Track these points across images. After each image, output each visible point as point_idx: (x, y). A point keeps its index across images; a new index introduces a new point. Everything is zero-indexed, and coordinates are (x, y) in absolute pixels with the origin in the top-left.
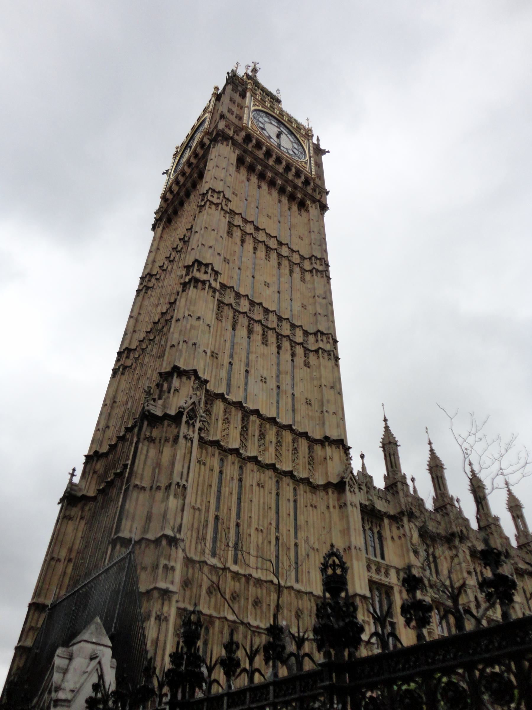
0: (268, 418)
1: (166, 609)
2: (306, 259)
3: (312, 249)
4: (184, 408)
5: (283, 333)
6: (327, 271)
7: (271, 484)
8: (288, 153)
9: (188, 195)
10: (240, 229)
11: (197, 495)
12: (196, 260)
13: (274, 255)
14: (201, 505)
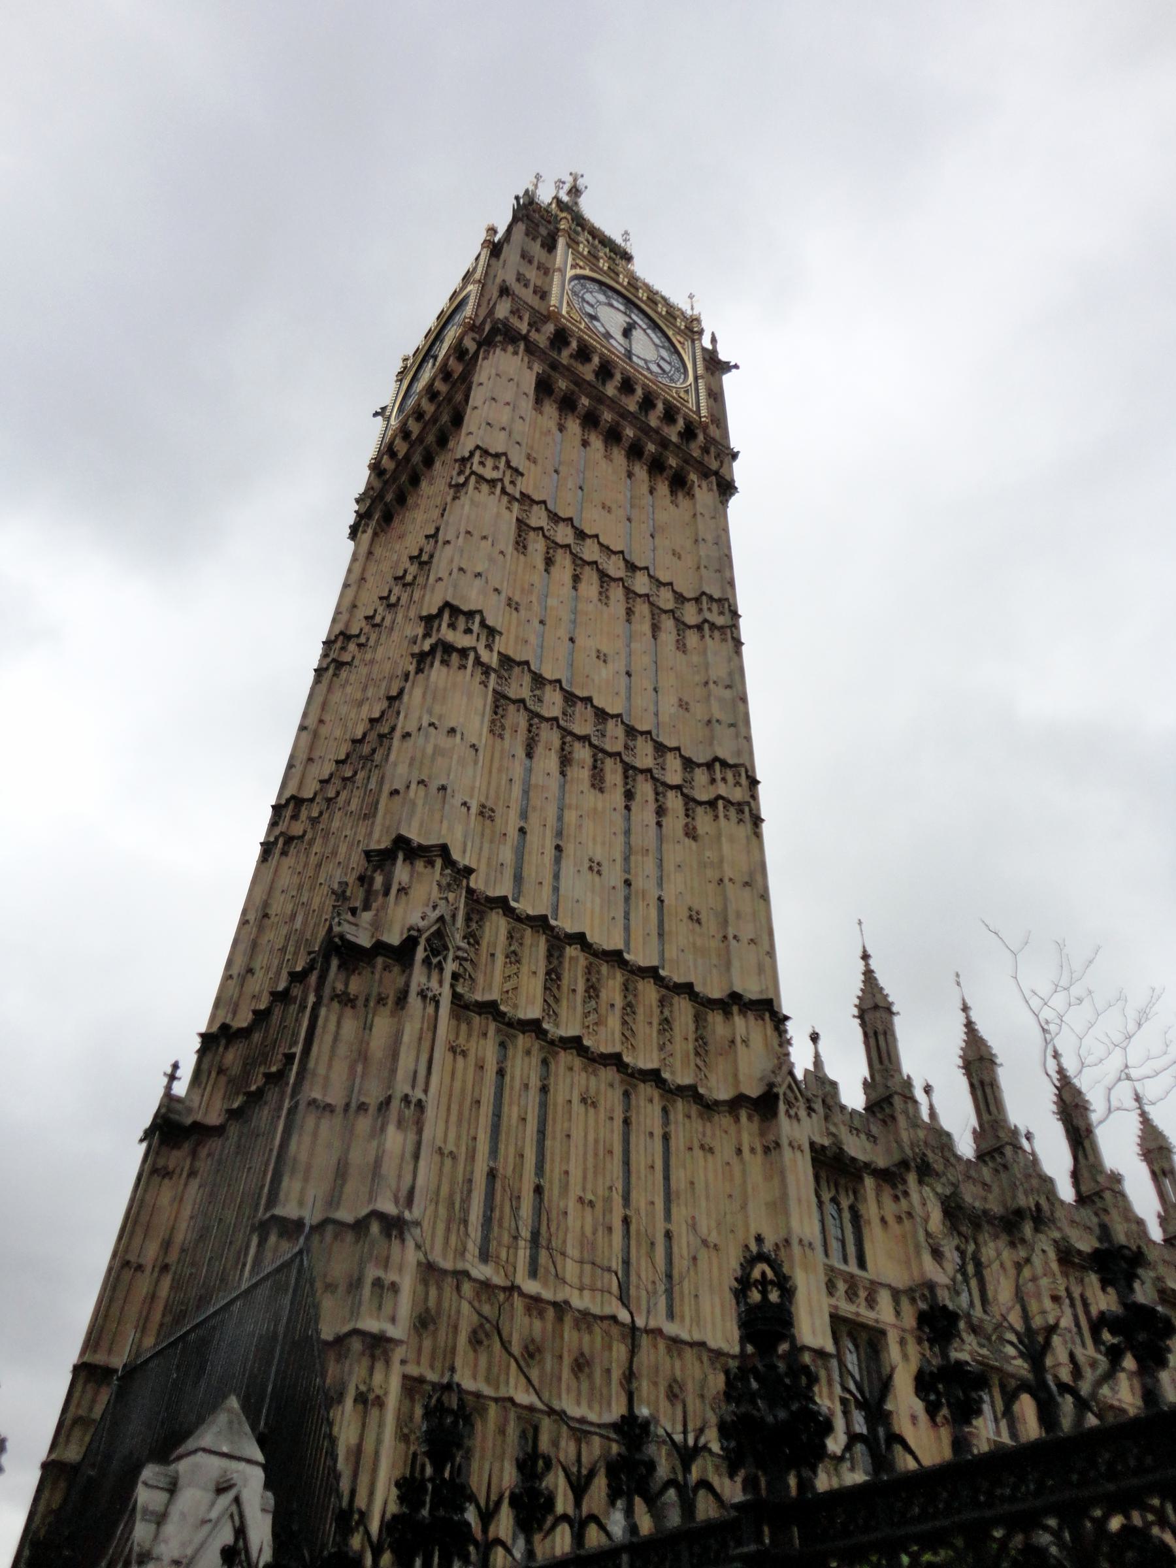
1: (378, 1377)
2: (689, 600)
3: (701, 578)
4: (419, 930)
5: (638, 765)
6: (735, 626)
7: (612, 1099)
8: (648, 369)
9: (429, 462)
10: (544, 536)
11: (447, 1121)
12: (447, 604)
13: (617, 593)
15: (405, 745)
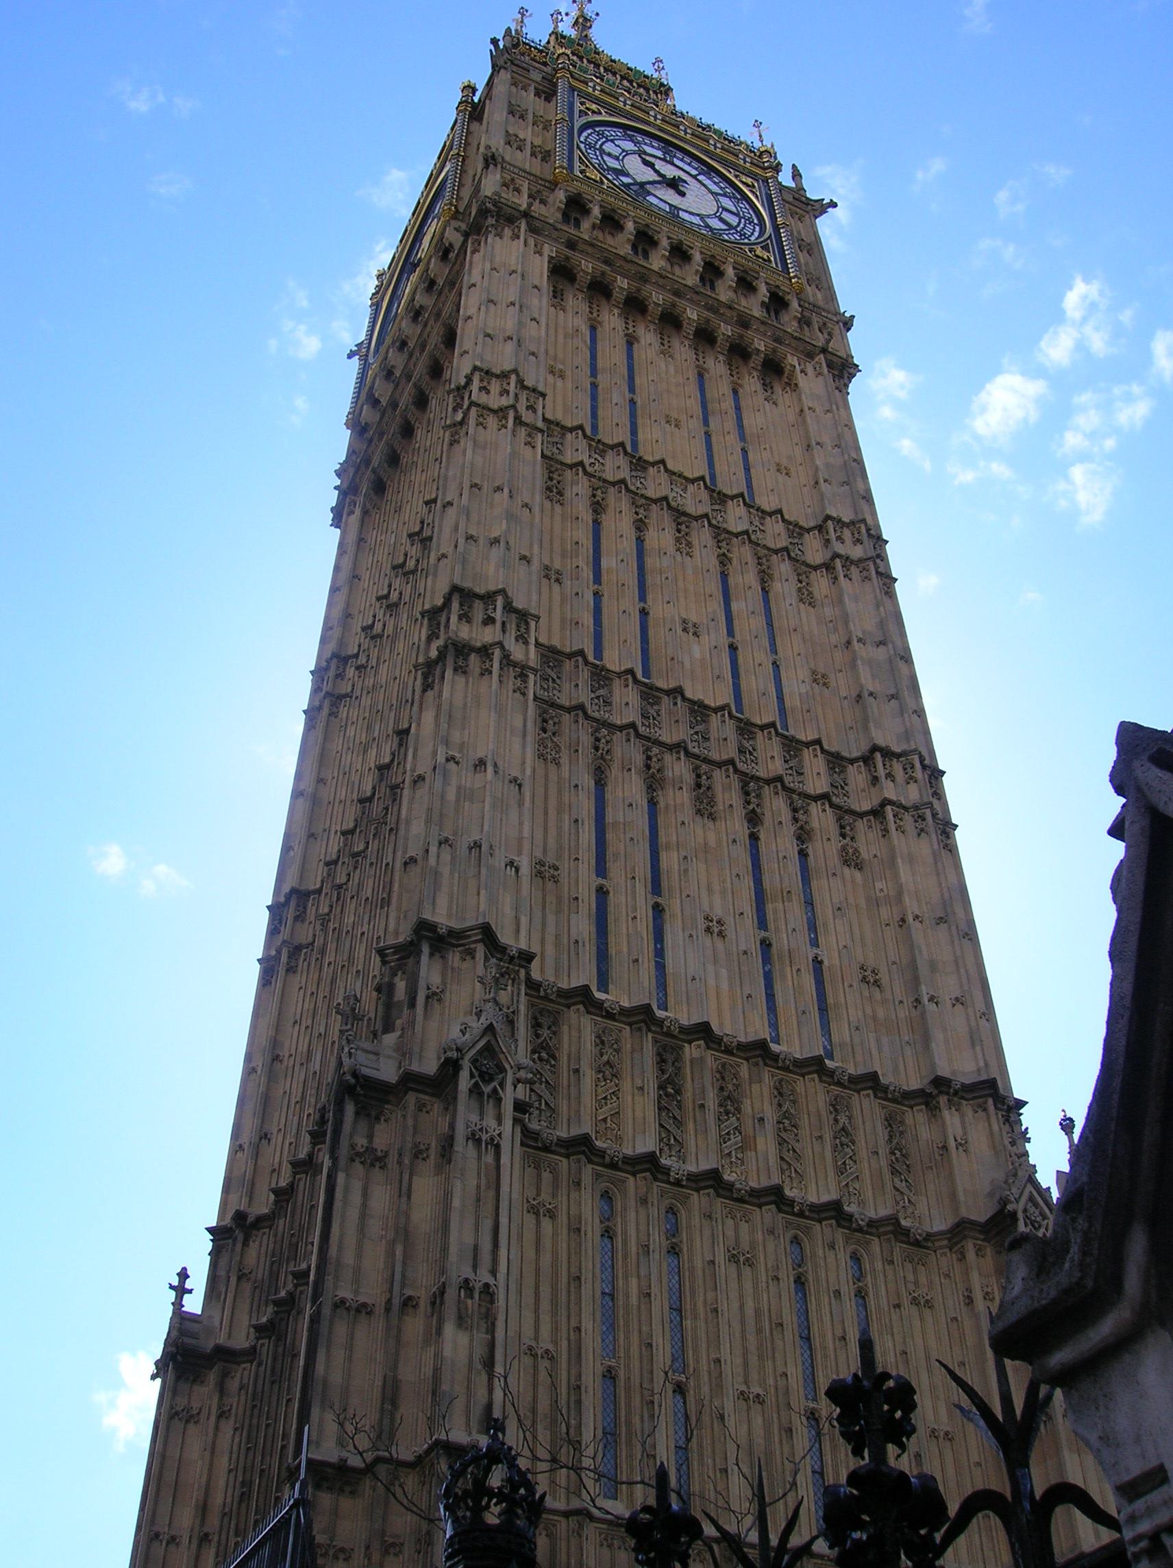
0: (741, 1047)
2: (808, 530)
3: (822, 496)
4: (458, 1050)
5: (762, 773)
6: (881, 557)
7: (773, 1252)
8: (707, 226)
9: (421, 401)
10: (585, 472)
11: (537, 1311)
13: (702, 536)
14: (555, 1342)
15: (419, 793)
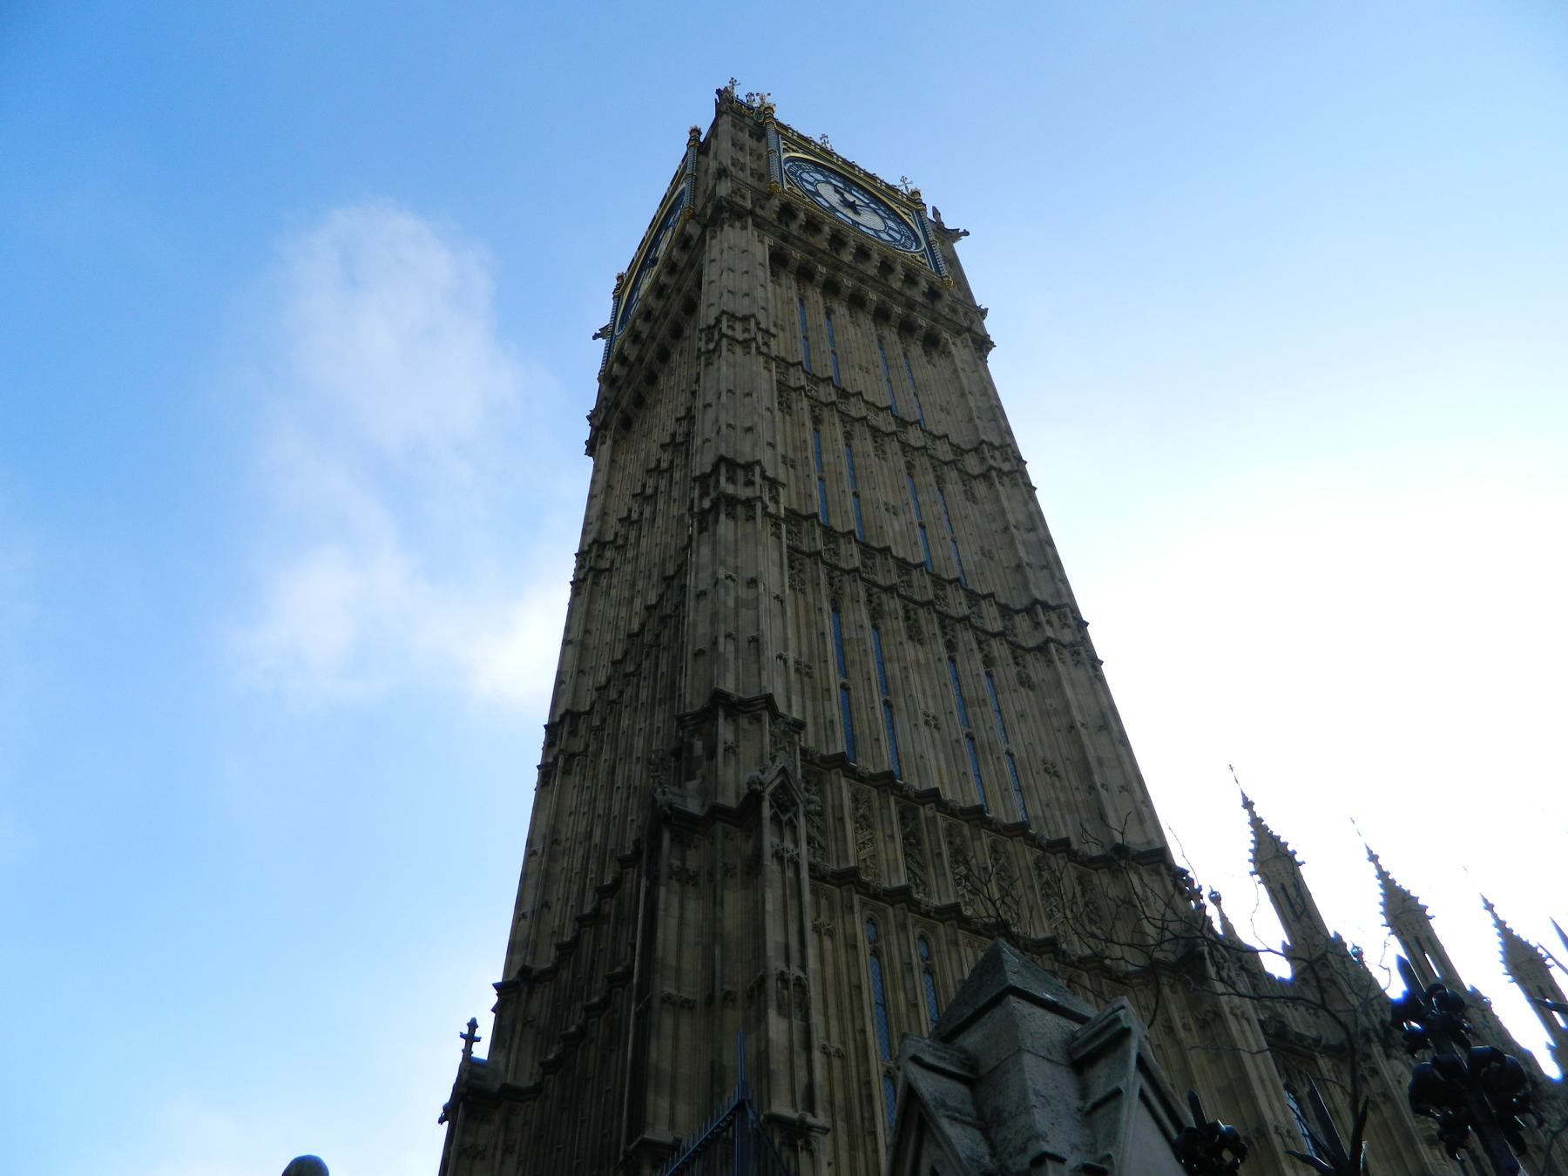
2: (968, 452)
3: (976, 428)
9: (664, 356)
12: (721, 459)
13: (893, 447)
14: (843, 1043)
15: (703, 603)
